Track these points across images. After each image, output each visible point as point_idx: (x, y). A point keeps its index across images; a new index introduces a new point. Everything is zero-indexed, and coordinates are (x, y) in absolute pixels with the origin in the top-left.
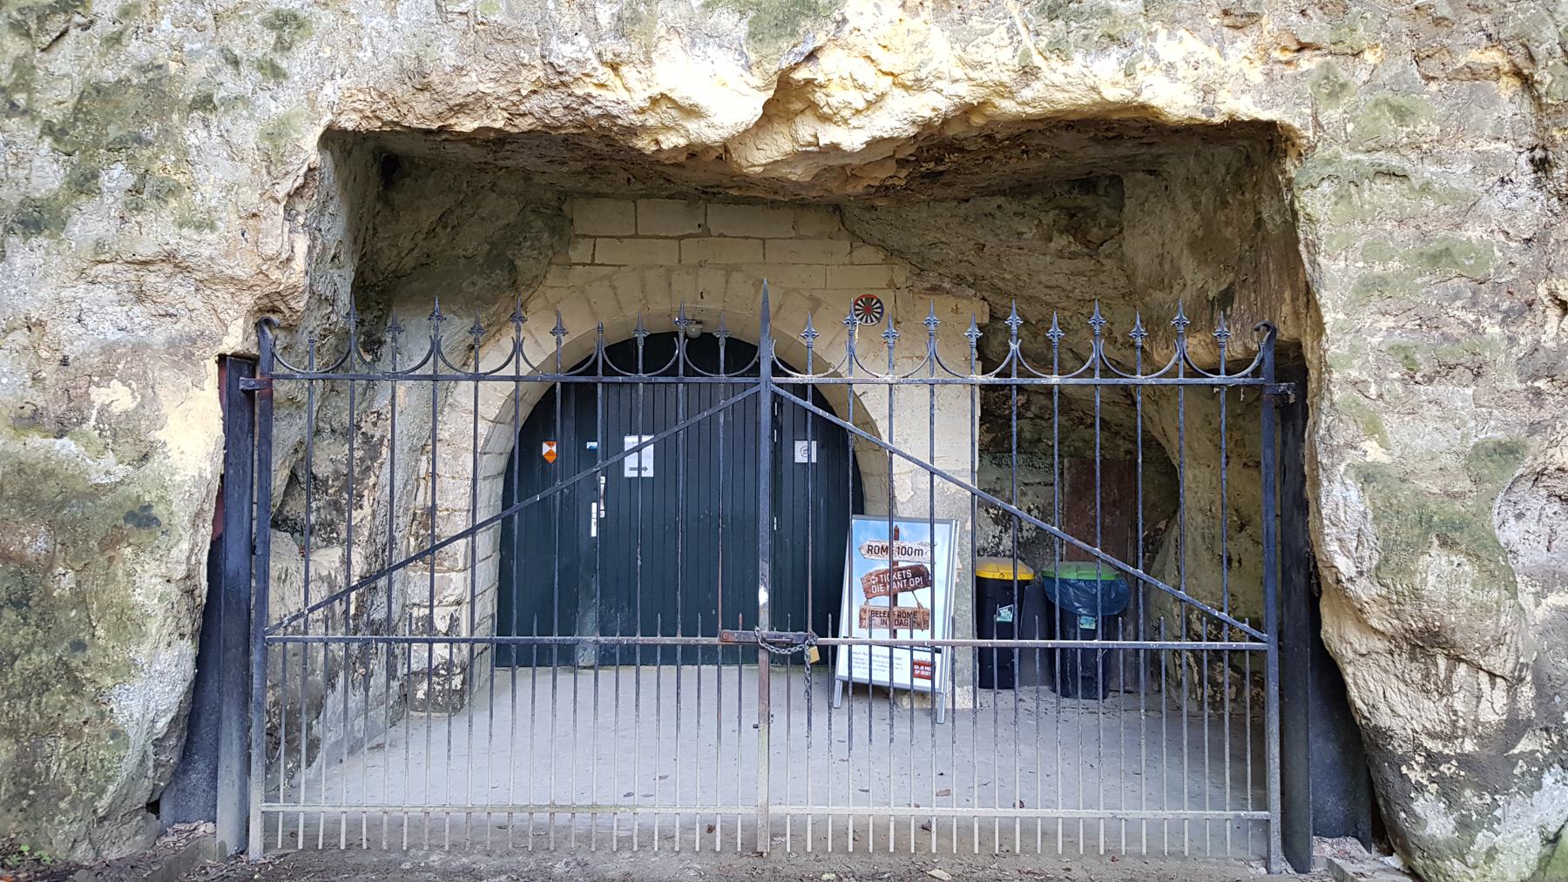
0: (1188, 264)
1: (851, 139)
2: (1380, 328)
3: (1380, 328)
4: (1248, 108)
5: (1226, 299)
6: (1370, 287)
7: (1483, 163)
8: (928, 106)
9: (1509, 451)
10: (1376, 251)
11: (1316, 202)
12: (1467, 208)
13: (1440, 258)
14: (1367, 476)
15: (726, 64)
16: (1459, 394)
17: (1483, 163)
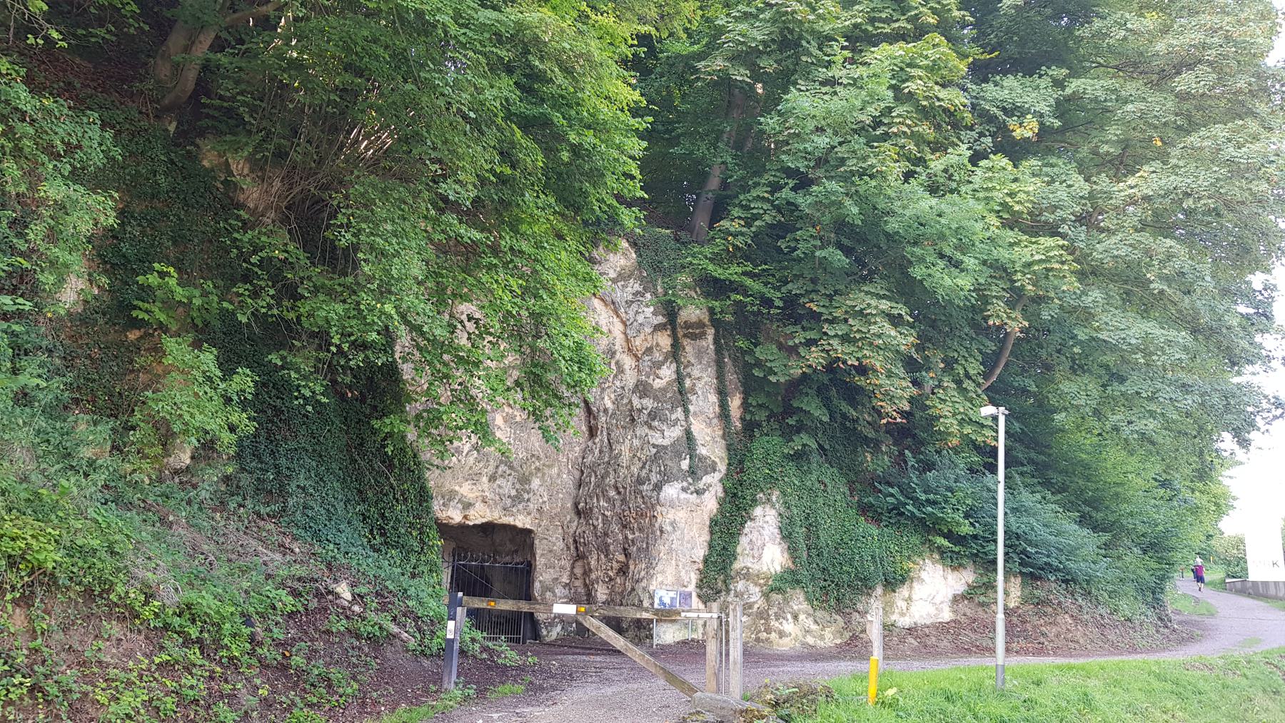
0: (508, 542)
1: (471, 523)
2: (543, 561)
3: (543, 561)
4: (528, 527)
5: (516, 551)
6: (542, 555)
7: (557, 538)
8: (484, 520)
9: (557, 579)
10: (543, 550)
11: (537, 542)
12: (555, 545)
13: (551, 551)
14: (540, 582)
15: (458, 512)
16: (552, 571)
17: (557, 538)
